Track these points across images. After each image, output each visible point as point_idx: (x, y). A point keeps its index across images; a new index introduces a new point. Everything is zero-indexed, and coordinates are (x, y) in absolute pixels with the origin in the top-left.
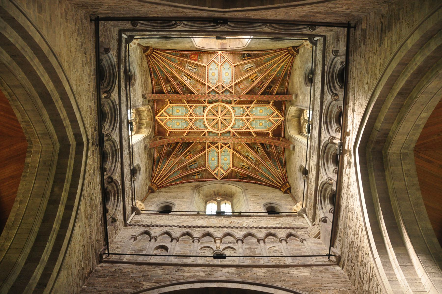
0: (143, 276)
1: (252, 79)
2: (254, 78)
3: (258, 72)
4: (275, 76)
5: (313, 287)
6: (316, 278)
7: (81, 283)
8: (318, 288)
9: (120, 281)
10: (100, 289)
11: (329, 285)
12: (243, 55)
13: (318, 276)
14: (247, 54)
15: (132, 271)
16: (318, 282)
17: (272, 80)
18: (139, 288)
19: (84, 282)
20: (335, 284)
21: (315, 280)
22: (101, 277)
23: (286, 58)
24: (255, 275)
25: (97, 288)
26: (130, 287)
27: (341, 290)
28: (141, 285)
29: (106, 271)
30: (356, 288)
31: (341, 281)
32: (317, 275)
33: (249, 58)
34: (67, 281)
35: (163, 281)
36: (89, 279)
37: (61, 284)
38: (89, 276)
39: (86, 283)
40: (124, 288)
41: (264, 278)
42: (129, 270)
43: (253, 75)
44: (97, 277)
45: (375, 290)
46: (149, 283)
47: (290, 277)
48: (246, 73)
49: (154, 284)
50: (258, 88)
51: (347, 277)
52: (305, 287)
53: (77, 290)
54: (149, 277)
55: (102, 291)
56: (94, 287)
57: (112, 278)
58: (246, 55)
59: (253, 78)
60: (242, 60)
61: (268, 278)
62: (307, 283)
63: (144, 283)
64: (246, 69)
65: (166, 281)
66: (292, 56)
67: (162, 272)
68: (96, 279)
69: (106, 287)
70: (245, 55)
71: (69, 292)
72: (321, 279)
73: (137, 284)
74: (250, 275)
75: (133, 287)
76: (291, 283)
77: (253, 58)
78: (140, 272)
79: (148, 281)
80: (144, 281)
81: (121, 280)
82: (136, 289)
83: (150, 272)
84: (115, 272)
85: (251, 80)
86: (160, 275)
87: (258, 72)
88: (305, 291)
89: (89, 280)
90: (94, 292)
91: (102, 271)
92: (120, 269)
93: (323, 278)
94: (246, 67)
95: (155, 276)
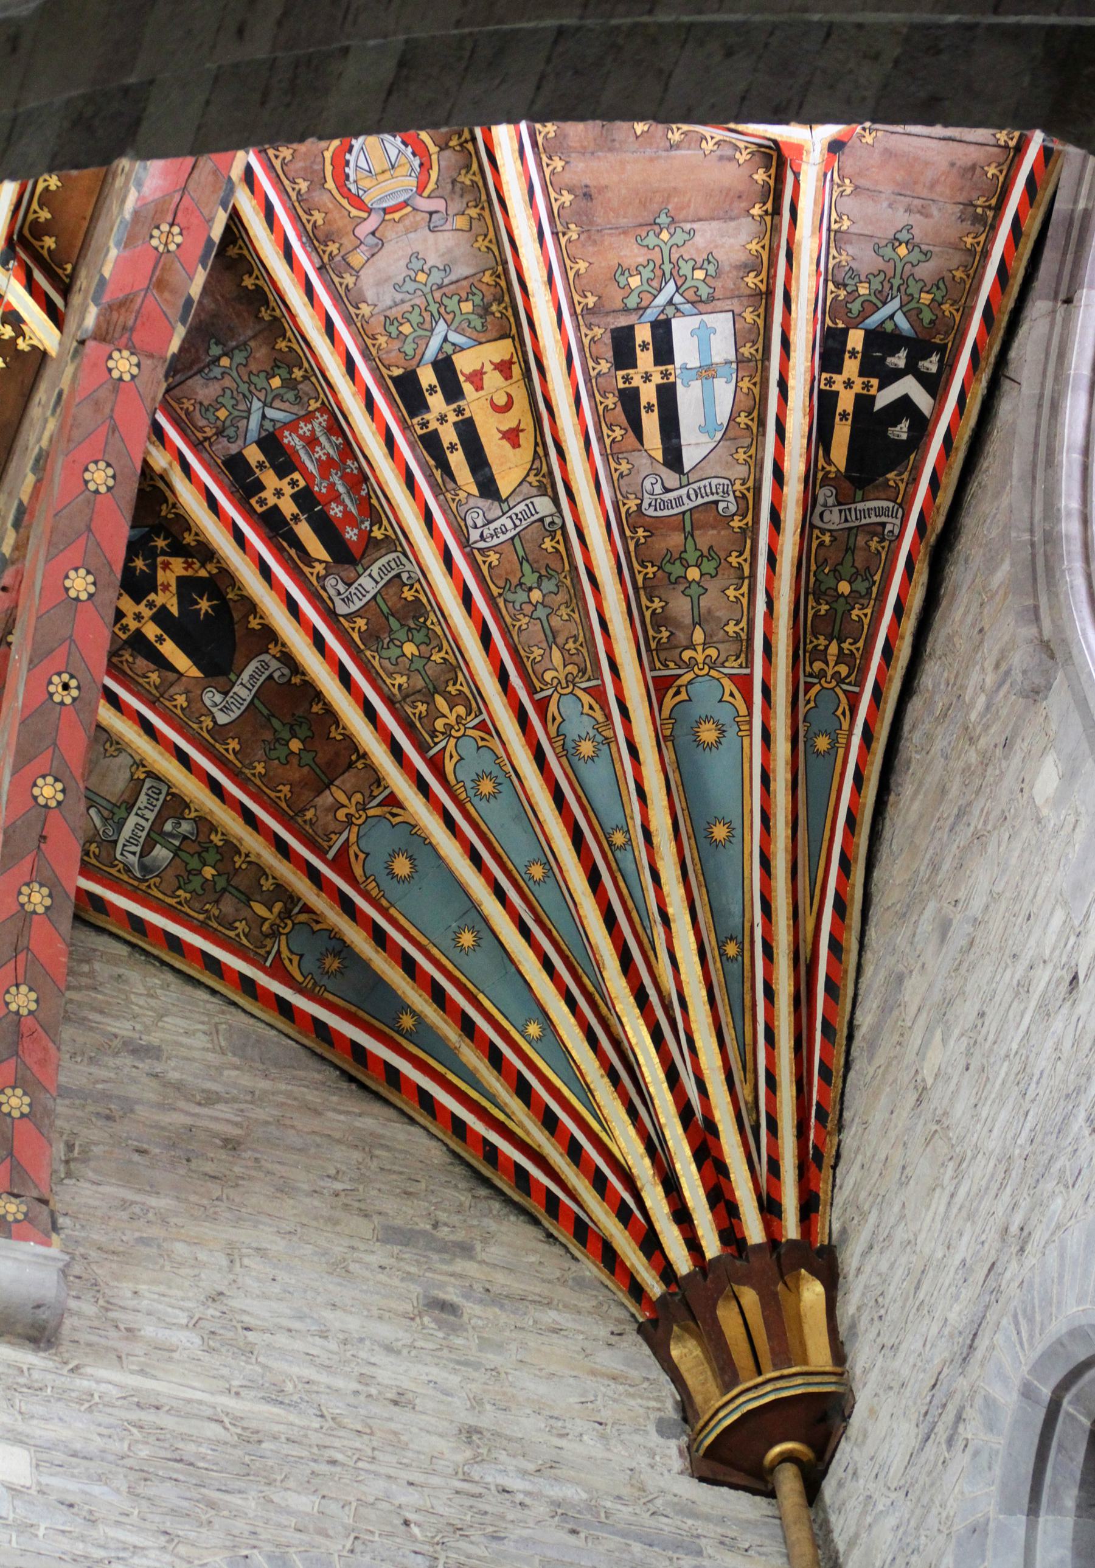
1: (452, 391)
2: (468, 431)
3: (554, 529)
4: (393, 801)
12: (919, 348)
14: (922, 426)
17: (331, 715)
23: (656, 1148)
33: (842, 433)
43: (520, 414)
48: (585, 316)
50: (270, 444)
58: (905, 405)
59: (475, 403)
60: (834, 309)
64: (662, 331)
66: (667, 1273)
70: (909, 387)
77: (809, 502)
85: (445, 368)
87: (554, 529)
94: (703, 336)
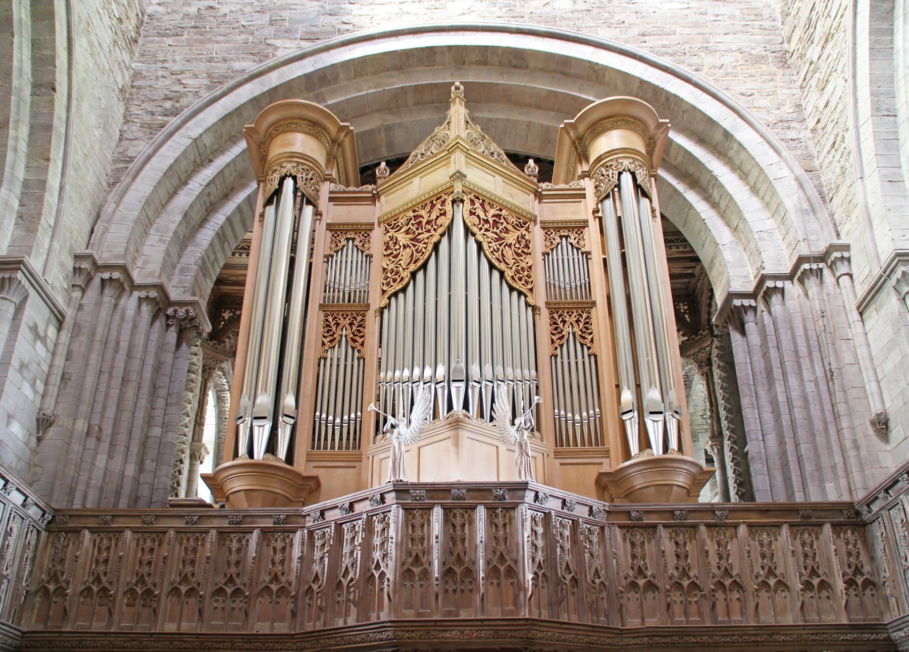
0: (272, 22)
5: (687, 43)
6: (700, 18)
7: (126, 57)
8: (700, 46)
9: (218, 42)
10: (176, 68)
11: (729, 38)
13: (705, 13)
15: (242, 10)
16: (702, 31)
18: (267, 56)
19: (131, 52)
20: (744, 37)
21: (694, 25)
22: (168, 36)
24: (548, 8)
25: (166, 65)
26: (244, 56)
27: (753, 52)
28: (270, 50)
29: (178, 17)
30: (791, 51)
31: (762, 28)
32: (703, 11)
34: (96, 63)
35: (322, 33)
36: (140, 42)
37: (84, 75)
38: (138, 33)
39: (137, 54)
40: (232, 59)
41: (570, 15)
42: (234, 9)
44: (159, 34)
45: (831, 65)
46: (289, 41)
47: (637, 12)
49: (304, 44)
51: (779, 18)
52: (666, 43)
53: (123, 77)
54: (287, 24)
55: (182, 72)
56: (160, 64)
57: (196, 34)
61: (580, 16)
62: (674, 33)
63: (278, 43)
65: (330, 34)
67: (318, 8)
68: (159, 42)
69: (188, 61)
71: (106, 86)
72: (711, 21)
73: (261, 47)
74: (536, 8)
75: (253, 54)
76: (636, 31)
78: (262, 12)
79: (286, 35)
80: (276, 37)
81: (221, 38)
82: (261, 61)
83: (285, 9)
84: (199, 16)
86: (312, 16)
88: (666, 53)
89: (143, 45)
90: (163, 77)
91: (166, 18)
92: (211, 8)
93: (717, 18)
95: (301, 21)
